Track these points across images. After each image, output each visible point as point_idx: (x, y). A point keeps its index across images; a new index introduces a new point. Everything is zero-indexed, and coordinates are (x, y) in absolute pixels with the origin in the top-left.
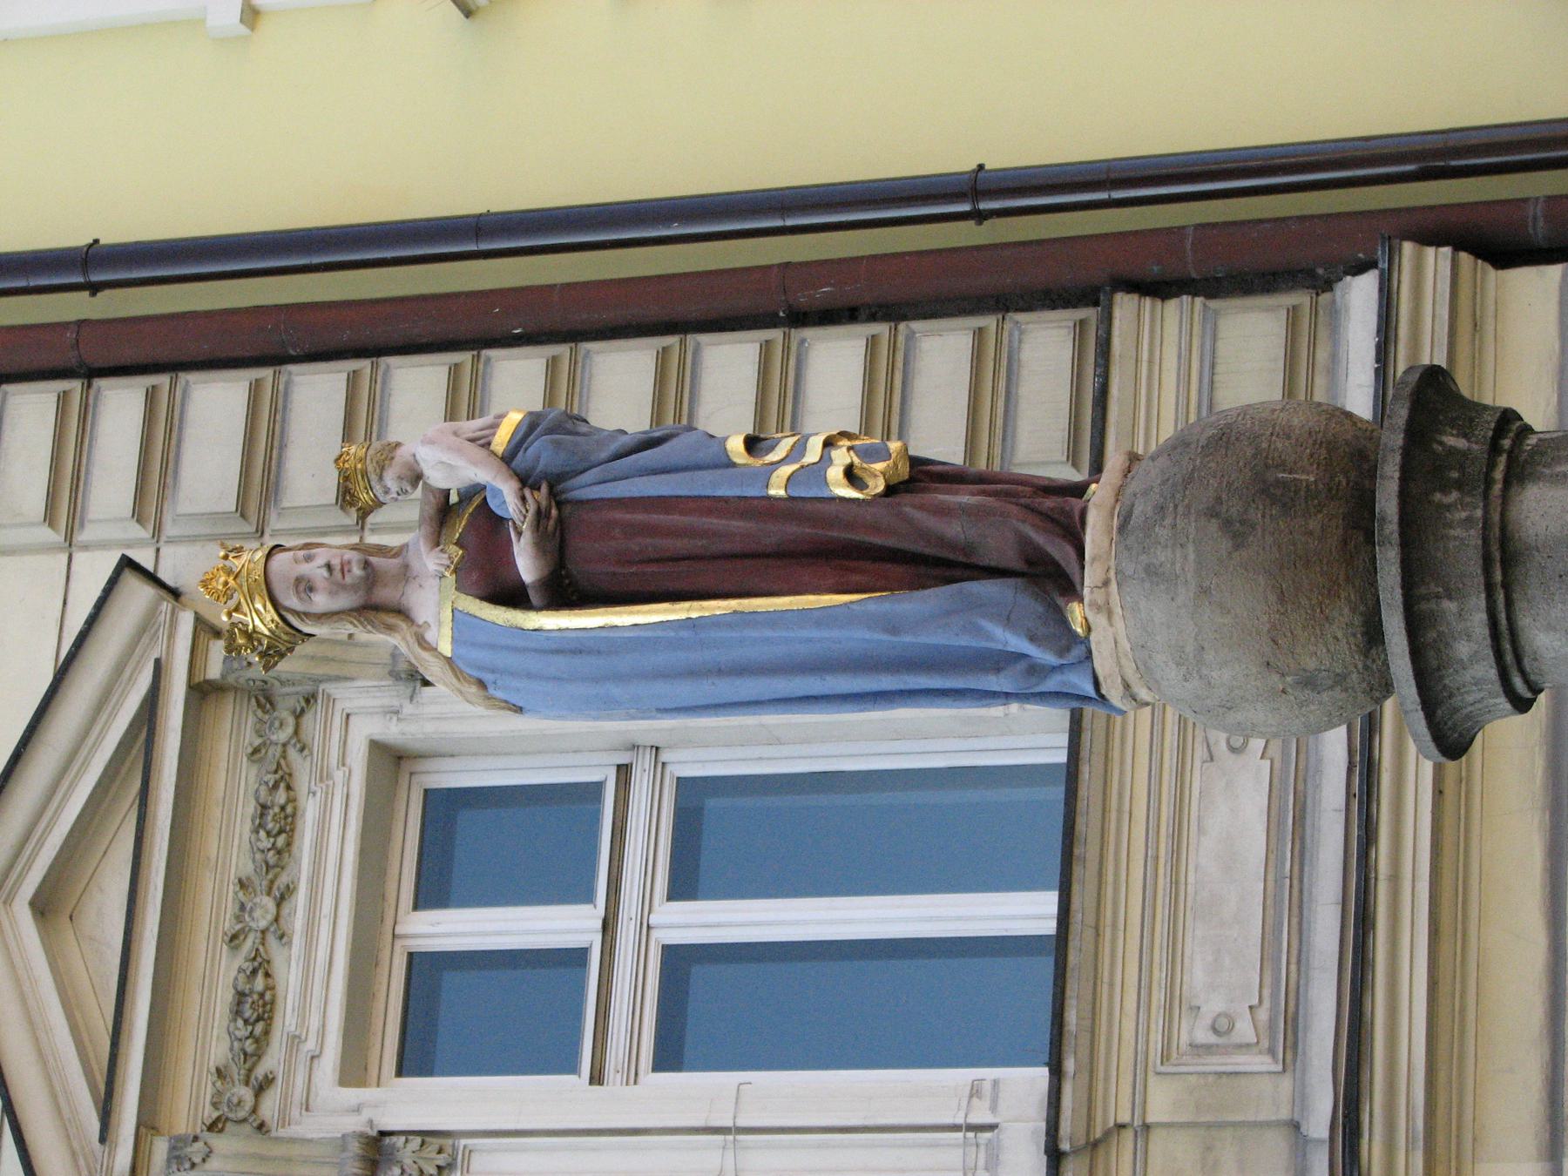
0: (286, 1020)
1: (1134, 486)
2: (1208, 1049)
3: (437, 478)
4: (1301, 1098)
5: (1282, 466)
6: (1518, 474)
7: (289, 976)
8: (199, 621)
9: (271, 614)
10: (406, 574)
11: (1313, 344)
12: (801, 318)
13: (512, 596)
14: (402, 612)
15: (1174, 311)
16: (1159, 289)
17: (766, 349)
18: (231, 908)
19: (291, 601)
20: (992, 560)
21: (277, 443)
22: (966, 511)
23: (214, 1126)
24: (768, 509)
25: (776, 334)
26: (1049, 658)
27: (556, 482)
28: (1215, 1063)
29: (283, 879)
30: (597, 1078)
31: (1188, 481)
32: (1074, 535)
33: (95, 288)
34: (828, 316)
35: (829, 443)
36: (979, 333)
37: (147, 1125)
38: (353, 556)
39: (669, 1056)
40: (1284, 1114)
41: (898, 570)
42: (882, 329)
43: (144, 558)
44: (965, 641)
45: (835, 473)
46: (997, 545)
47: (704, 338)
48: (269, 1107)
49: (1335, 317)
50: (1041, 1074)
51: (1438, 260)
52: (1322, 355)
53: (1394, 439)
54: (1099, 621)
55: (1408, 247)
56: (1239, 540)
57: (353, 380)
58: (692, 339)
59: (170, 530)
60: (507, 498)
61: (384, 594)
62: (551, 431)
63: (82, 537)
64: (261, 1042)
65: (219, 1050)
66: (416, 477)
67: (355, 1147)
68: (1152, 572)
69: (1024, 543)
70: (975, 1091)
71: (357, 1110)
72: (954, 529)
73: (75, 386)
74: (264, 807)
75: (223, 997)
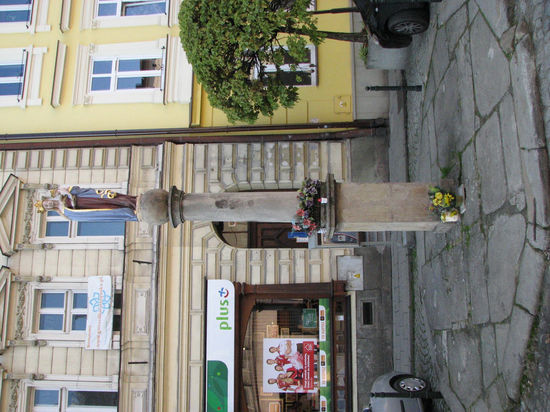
0: (32, 230)
1: (142, 198)
2: (142, 234)
3: (62, 194)
4: (153, 240)
5: (158, 197)
6: (183, 199)
7: (32, 225)
8: (20, 181)
9: (43, 209)
10: (58, 204)
11: (155, 151)
12: (94, 147)
13: (71, 207)
14: (58, 208)
15: (139, 148)
16: (137, 145)
17: (91, 150)
18: (25, 216)
19: (45, 207)
20: (126, 205)
21: (30, 159)
22: (123, 200)
23: (24, 243)
24: (101, 199)
25: (92, 149)
26: (132, 217)
27: (76, 195)
28: (143, 236)
29: (31, 213)
30: (70, 237)
31: (148, 198)
32: (135, 203)
33: (7, 140)
34: (98, 147)
35: (108, 192)
36: (116, 149)
37: (15, 243)
38: (52, 202)
39: (79, 234)
40: (151, 242)
41: (115, 206)
42: (105, 148)
43: (13, 173)
44: (123, 214)
45: (108, 195)
46: (127, 203)
47: (83, 149)
48: (30, 240)
49: (158, 149)
50: (123, 237)
51: (170, 143)
52: (156, 153)
53: (170, 195)
54: (138, 213)
55: (166, 142)
56: (153, 206)
57: (40, 152)
58: (81, 149)
59: (16, 170)
60: (70, 196)
61: (56, 206)
62: (76, 189)
63: (6, 170)
64: (29, 232)
65: (24, 234)
66: (60, 194)
67: (41, 245)
68: (144, 208)
69: (130, 204)
70: (115, 239)
71: (41, 241)
72: (122, 202)
73: (4, 152)
74: (29, 204)
75: (24, 227)
